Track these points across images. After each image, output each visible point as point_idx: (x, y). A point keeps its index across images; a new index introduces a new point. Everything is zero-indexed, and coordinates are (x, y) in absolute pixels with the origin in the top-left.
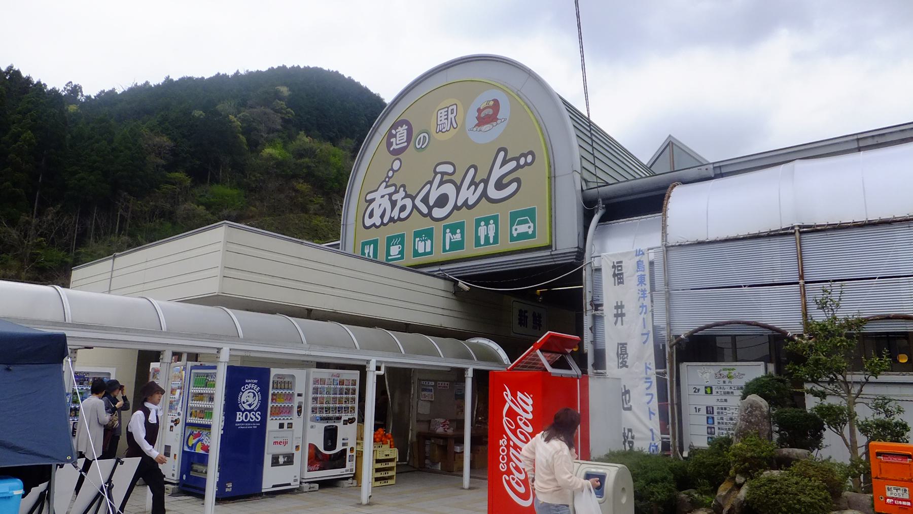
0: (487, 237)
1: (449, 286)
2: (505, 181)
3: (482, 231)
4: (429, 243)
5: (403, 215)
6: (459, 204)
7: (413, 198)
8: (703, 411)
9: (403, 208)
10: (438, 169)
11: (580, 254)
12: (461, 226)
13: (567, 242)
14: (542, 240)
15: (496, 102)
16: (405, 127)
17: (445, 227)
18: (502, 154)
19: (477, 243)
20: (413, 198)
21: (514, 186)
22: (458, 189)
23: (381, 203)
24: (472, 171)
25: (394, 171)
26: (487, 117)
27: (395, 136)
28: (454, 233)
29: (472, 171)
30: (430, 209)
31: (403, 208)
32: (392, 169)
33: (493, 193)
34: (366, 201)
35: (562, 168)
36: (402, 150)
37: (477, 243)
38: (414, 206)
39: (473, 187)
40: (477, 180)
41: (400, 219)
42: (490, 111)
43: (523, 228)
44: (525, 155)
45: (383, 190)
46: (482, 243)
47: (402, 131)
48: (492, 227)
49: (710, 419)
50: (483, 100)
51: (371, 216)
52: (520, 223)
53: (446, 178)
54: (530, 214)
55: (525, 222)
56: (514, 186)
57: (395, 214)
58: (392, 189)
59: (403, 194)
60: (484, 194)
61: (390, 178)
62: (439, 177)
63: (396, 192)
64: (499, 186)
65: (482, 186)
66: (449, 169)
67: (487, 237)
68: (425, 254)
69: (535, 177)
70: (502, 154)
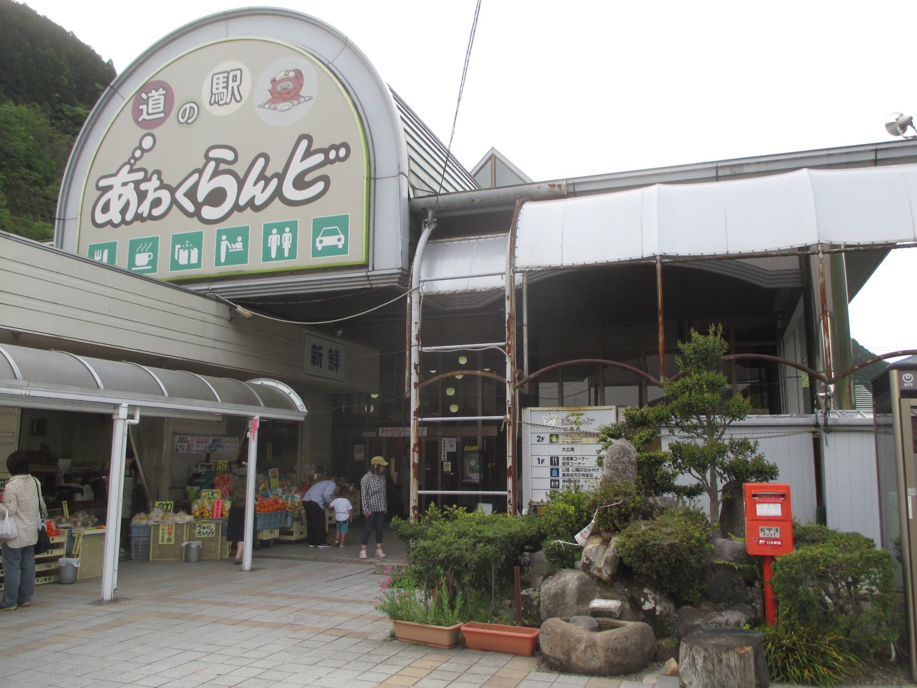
0: (280, 249)
1: (223, 310)
2: (308, 178)
3: (274, 241)
4: (195, 252)
5: (156, 212)
6: (242, 202)
7: (173, 191)
8: (547, 462)
9: (157, 203)
10: (213, 154)
11: (405, 275)
12: (244, 232)
13: (388, 260)
14: (356, 255)
15: (299, 75)
16: (161, 91)
17: (220, 233)
18: (304, 144)
19: (267, 256)
20: (173, 191)
21: (320, 186)
22: (241, 183)
23: (121, 192)
24: (261, 162)
25: (144, 151)
26: (287, 91)
28: (232, 240)
29: (261, 162)
30: (198, 206)
31: (157, 203)
32: (140, 147)
33: (289, 191)
34: (98, 188)
35: (385, 166)
36: (157, 123)
37: (267, 256)
38: (174, 201)
39: (262, 183)
40: (268, 173)
41: (151, 217)
42: (290, 85)
43: (330, 241)
44: (336, 148)
45: (124, 175)
46: (273, 255)
47: (157, 96)
48: (287, 236)
49: (554, 471)
50: (280, 68)
51: (106, 209)
52: (328, 233)
53: (223, 166)
54: (341, 224)
55: (335, 233)
56: (320, 186)
57: (145, 209)
58: (140, 176)
59: (157, 184)
60: (278, 193)
61: (136, 159)
62: (212, 165)
63: (147, 179)
64: (300, 183)
65: (274, 183)
66: (230, 156)
67: (280, 249)
68: (189, 266)
69: (348, 178)
70: (304, 144)
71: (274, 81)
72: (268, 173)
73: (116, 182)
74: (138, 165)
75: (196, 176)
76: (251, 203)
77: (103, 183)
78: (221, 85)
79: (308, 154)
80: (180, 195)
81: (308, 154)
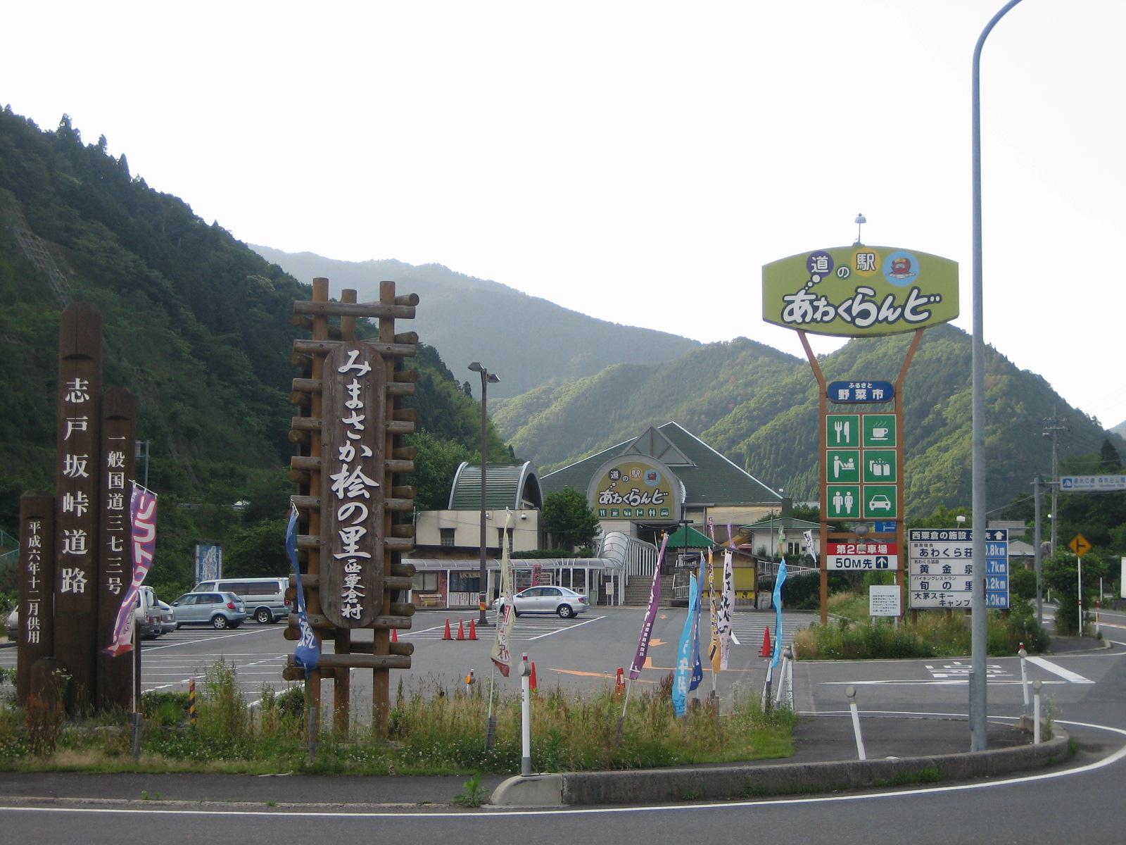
2: (919, 310)
9: (825, 313)
10: (859, 290)
18: (916, 291)
20: (836, 309)
21: (925, 315)
22: (879, 309)
25: (814, 283)
27: (816, 262)
29: (890, 299)
33: (908, 315)
38: (837, 314)
39: (892, 310)
40: (896, 304)
45: (802, 295)
53: (866, 298)
57: (818, 316)
59: (826, 303)
61: (809, 288)
65: (899, 310)
66: (871, 293)
70: (916, 291)
71: (893, 262)
72: (896, 304)
73: (797, 298)
74: (811, 291)
75: (850, 301)
76: (886, 319)
77: (787, 298)
78: (863, 260)
79: (918, 297)
80: (841, 311)
81: (918, 297)
